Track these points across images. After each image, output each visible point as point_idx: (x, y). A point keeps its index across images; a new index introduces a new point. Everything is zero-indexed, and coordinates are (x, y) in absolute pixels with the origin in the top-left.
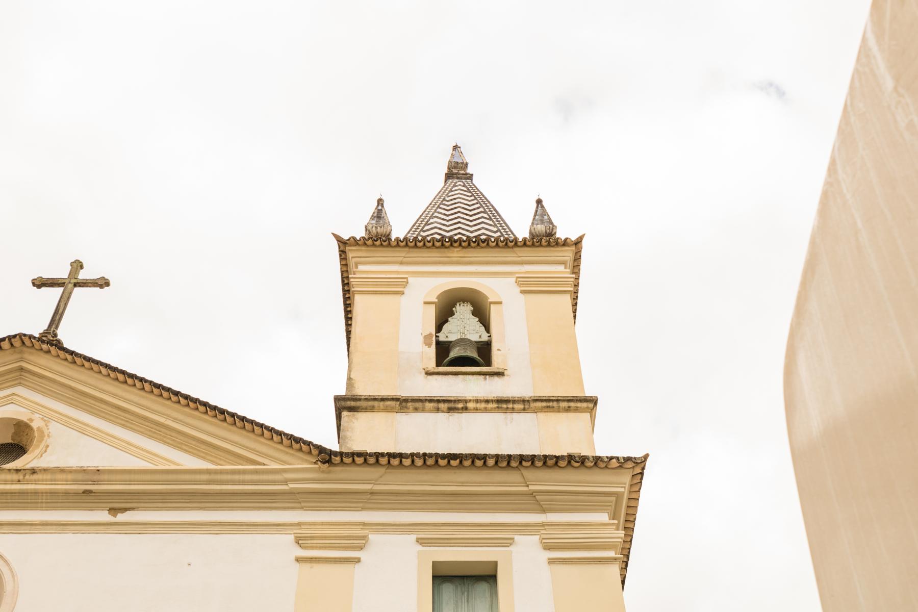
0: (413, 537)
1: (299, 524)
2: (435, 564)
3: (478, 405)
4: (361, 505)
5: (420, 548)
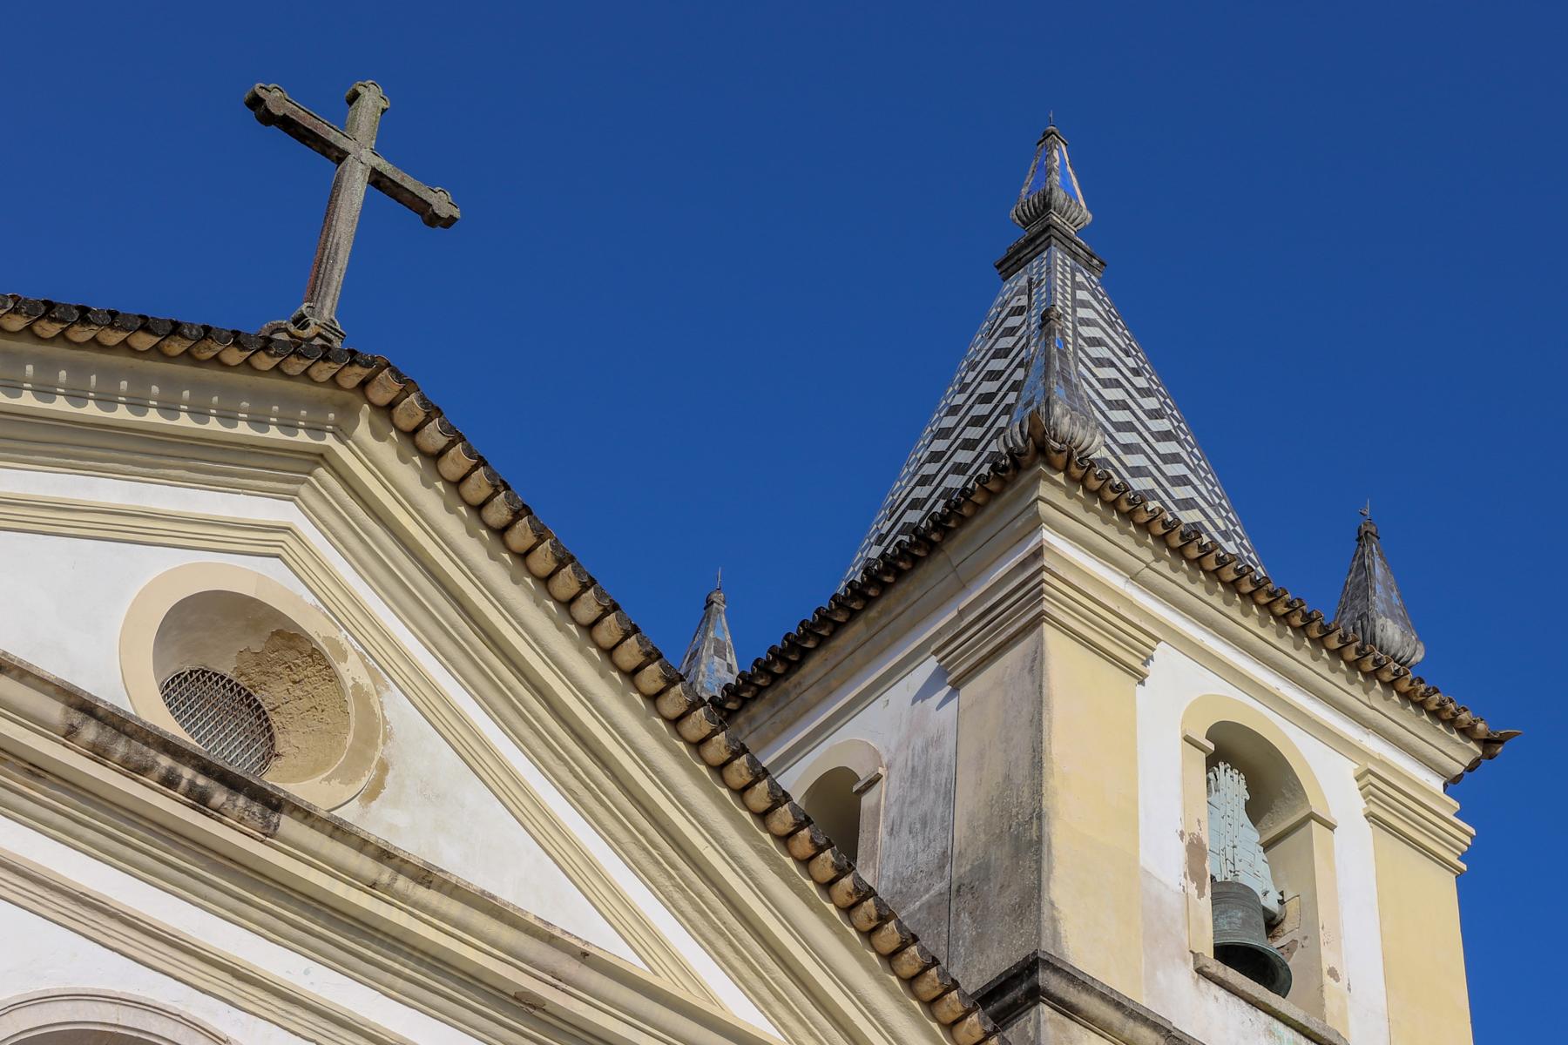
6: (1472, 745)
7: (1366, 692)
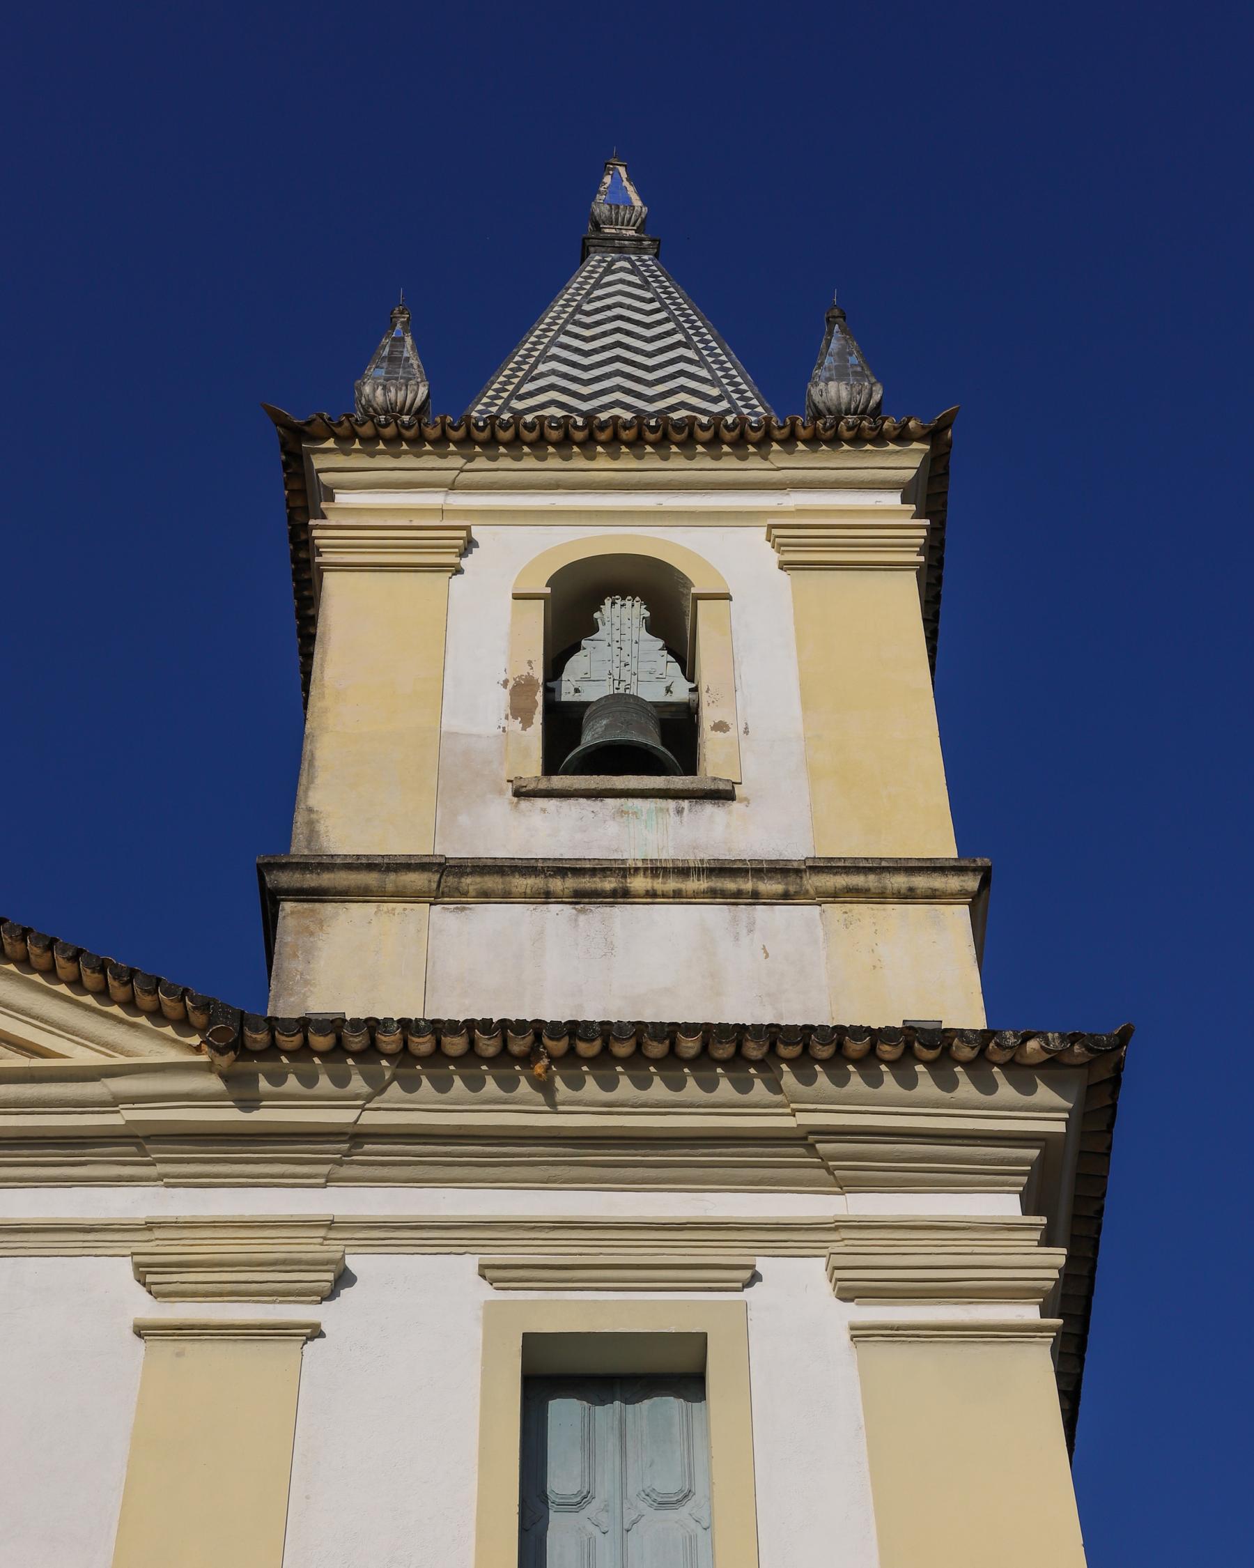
0: (470, 1263)
1: (150, 1226)
2: (531, 1342)
3: (659, 885)
4: (324, 1169)
5: (488, 1293)
6: (915, 445)
7: (766, 459)
